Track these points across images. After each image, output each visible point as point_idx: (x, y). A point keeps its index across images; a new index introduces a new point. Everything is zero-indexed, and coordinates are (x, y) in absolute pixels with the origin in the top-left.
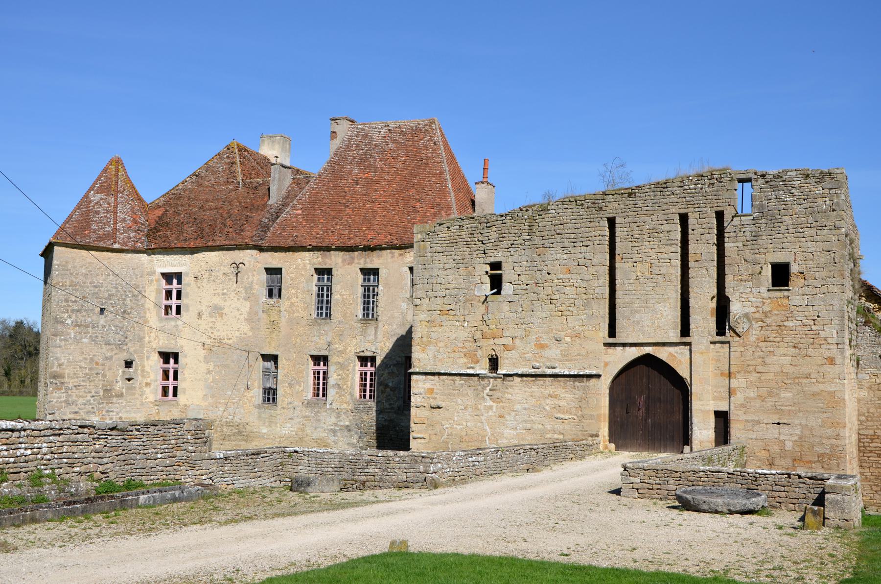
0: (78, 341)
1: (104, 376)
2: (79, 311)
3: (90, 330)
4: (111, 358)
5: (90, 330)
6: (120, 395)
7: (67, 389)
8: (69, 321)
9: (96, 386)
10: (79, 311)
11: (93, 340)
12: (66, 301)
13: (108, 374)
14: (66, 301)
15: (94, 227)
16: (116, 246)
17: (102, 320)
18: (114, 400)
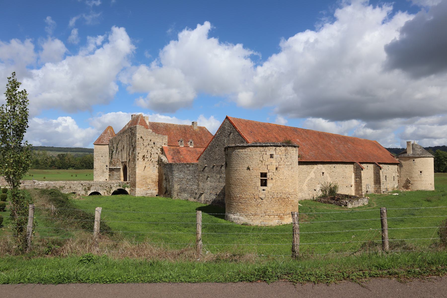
0: (98, 162)
1: (102, 168)
2: (98, 156)
3: (100, 160)
4: (103, 165)
5: (100, 160)
6: (105, 172)
7: (97, 171)
8: (97, 159)
9: (101, 170)
10: (98, 156)
11: (100, 162)
12: (96, 155)
13: (103, 168)
14: (96, 155)
15: (101, 140)
16: (104, 144)
17: (102, 158)
18: (104, 173)
